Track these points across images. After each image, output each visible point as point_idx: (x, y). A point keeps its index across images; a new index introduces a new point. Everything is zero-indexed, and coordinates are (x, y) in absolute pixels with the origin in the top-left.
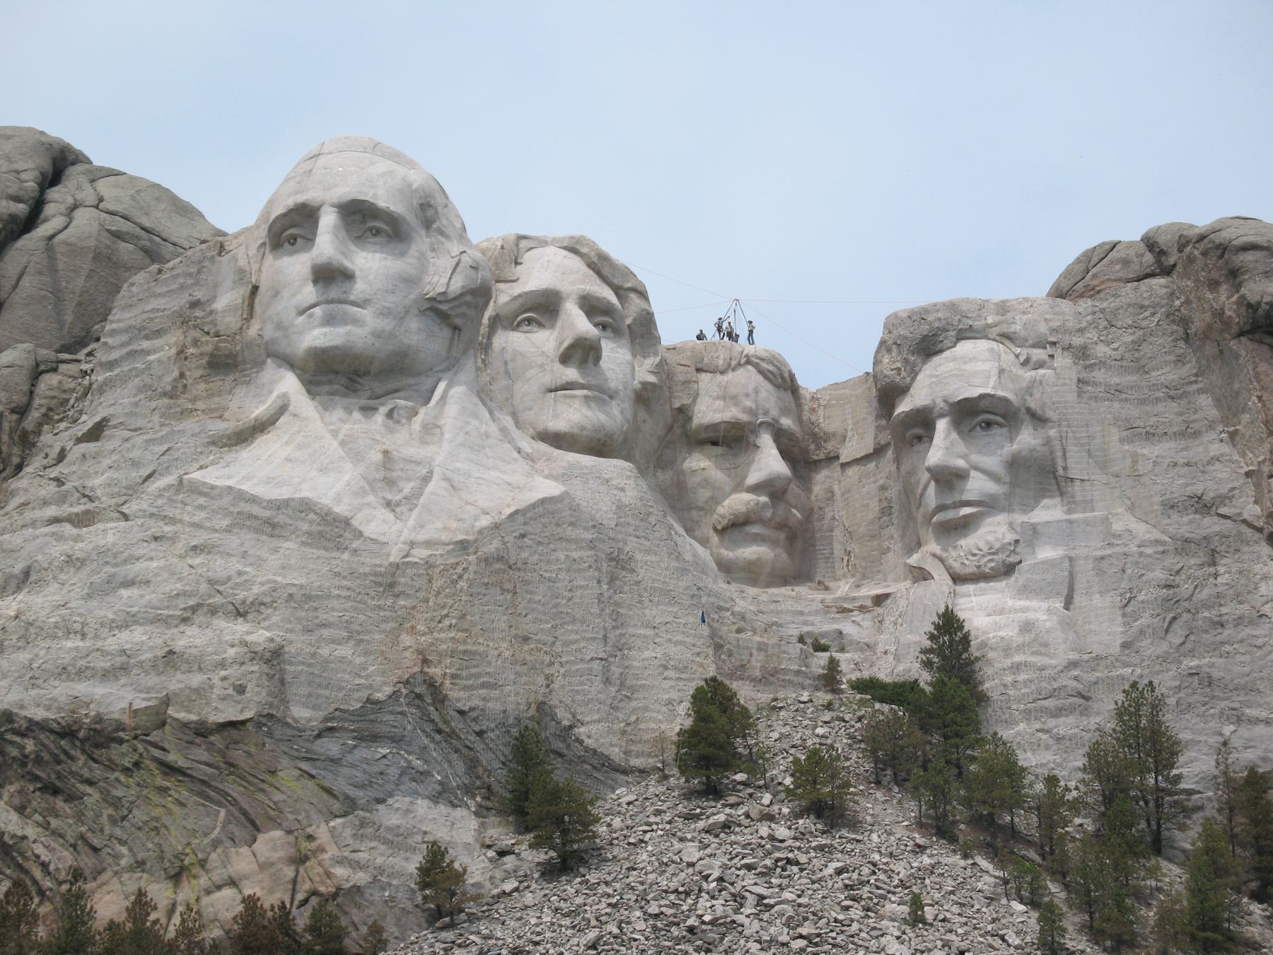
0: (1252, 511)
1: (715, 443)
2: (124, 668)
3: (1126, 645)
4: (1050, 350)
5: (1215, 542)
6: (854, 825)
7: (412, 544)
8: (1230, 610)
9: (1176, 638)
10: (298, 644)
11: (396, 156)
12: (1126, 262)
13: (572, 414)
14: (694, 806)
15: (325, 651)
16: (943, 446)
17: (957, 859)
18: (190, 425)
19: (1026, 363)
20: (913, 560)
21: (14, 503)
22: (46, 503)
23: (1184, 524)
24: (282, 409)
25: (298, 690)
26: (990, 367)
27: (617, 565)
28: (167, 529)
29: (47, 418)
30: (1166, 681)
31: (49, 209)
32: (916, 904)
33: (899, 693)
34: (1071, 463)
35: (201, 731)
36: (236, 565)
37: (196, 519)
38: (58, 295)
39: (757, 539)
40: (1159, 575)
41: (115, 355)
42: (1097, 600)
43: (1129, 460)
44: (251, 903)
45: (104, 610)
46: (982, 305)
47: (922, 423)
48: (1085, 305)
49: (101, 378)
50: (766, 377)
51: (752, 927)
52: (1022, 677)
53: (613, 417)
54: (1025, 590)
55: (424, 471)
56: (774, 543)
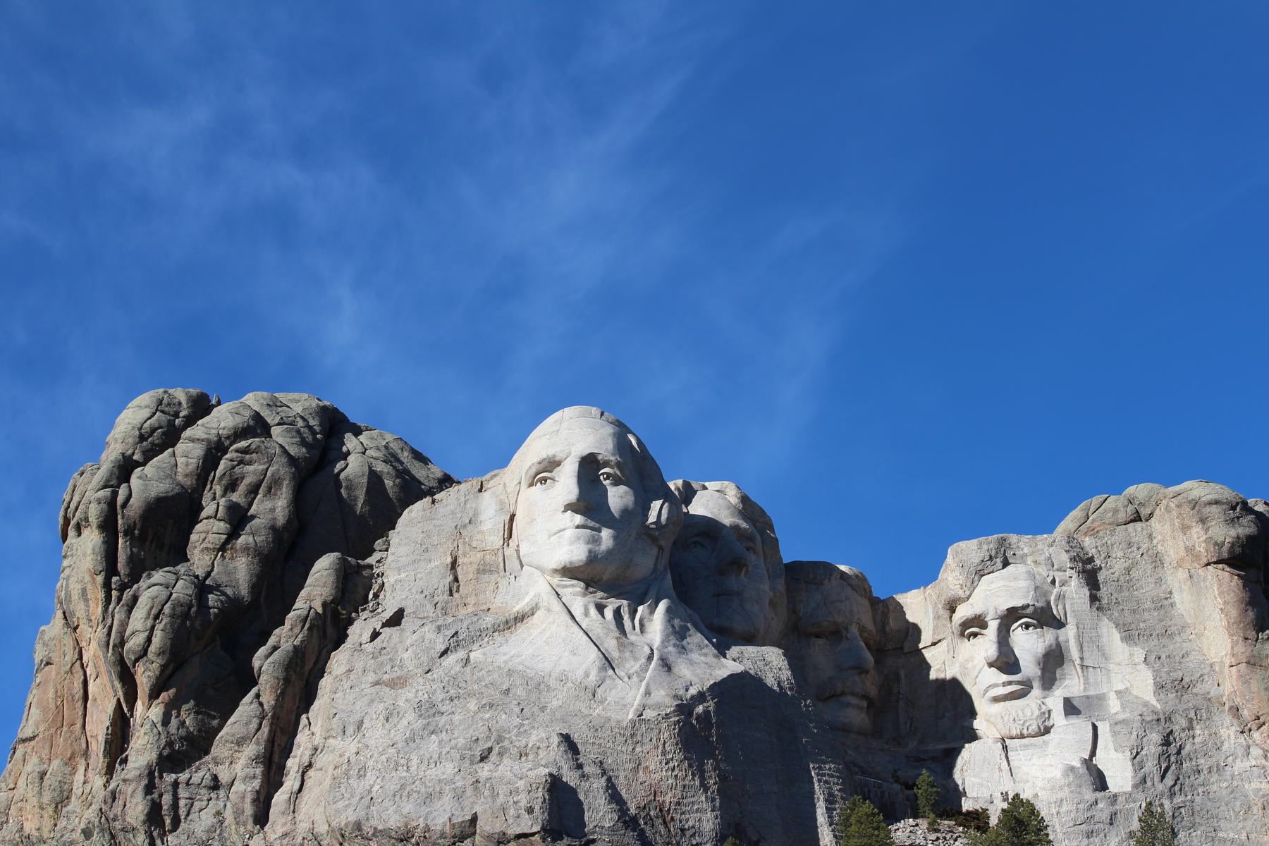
1: (817, 636)
3: (1135, 786)
4: (1069, 573)
5: (1192, 715)
9: (1169, 780)
12: (1116, 511)
19: (1053, 582)
34: (1086, 655)
39: (848, 705)
40: (1155, 737)
42: (1113, 754)
43: (1127, 654)
49: (392, 580)
50: (854, 589)
52: (1064, 809)
55: (648, 651)
56: (860, 708)
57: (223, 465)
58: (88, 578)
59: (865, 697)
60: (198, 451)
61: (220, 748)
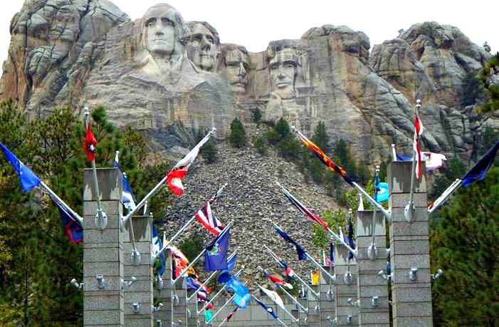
0: (343, 88)
1: (231, 65)
2: (119, 117)
7: (176, 93)
11: (171, 7)
13: (206, 62)
14: (235, 150)
15: (160, 115)
17: (286, 163)
20: (273, 93)
21: (91, 79)
22: (98, 79)
24: (148, 61)
27: (217, 97)
28: (126, 87)
29: (96, 59)
30: (326, 124)
31: (90, 8)
32: (281, 172)
33: (270, 123)
36: (141, 96)
37: (132, 84)
39: (239, 86)
41: (110, 46)
45: (115, 104)
46: (289, 40)
47: (277, 65)
48: (310, 41)
51: (250, 177)
56: (242, 87)
58: (18, 48)
59: (243, 83)
60: (51, 9)
61: (57, 102)
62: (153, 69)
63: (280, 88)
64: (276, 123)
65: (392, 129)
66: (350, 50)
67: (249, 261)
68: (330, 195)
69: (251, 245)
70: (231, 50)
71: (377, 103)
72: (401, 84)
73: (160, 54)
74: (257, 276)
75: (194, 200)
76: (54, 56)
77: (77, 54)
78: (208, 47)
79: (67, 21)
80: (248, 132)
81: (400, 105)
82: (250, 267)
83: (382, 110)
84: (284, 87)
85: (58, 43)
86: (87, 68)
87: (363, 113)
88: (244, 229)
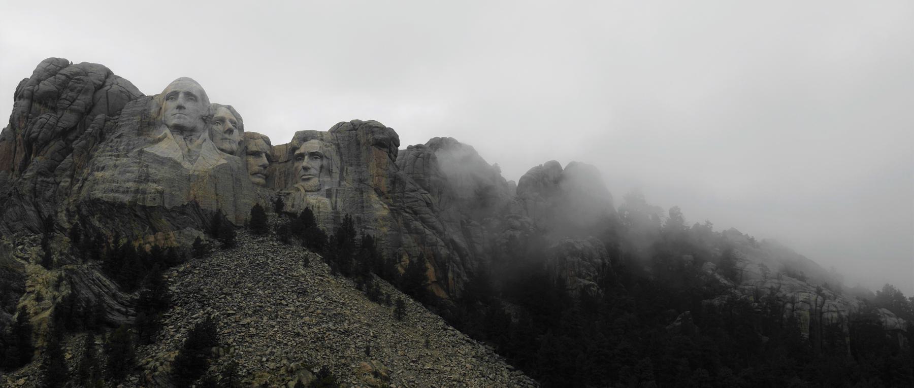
0: (371, 183)
2: (127, 192)
6: (290, 243)
8: (365, 204)
10: (167, 190)
16: (306, 162)
18: (143, 137)
23: (356, 185)
24: (165, 136)
25: (167, 201)
26: (318, 146)
35: (144, 208)
36: (154, 171)
38: (108, 103)
40: (351, 195)
44: (155, 249)
47: (302, 156)
51: (271, 264)
53: (235, 147)
54: (322, 195)
57: (71, 83)
60: (63, 77)
62: (168, 147)
63: (304, 180)
64: (299, 215)
65: (422, 227)
66: (380, 144)
67: (272, 353)
68: (360, 289)
69: (275, 335)
70: (255, 139)
71: (405, 200)
72: (425, 189)
73: (179, 129)
74: (282, 371)
75: (206, 284)
76: (60, 124)
77: (85, 127)
78: (230, 131)
79: (80, 92)
80: (270, 220)
81: (428, 204)
82: (273, 361)
83: (411, 208)
84: (308, 179)
85: (67, 114)
86: (96, 139)
87: (391, 210)
88: (265, 318)
